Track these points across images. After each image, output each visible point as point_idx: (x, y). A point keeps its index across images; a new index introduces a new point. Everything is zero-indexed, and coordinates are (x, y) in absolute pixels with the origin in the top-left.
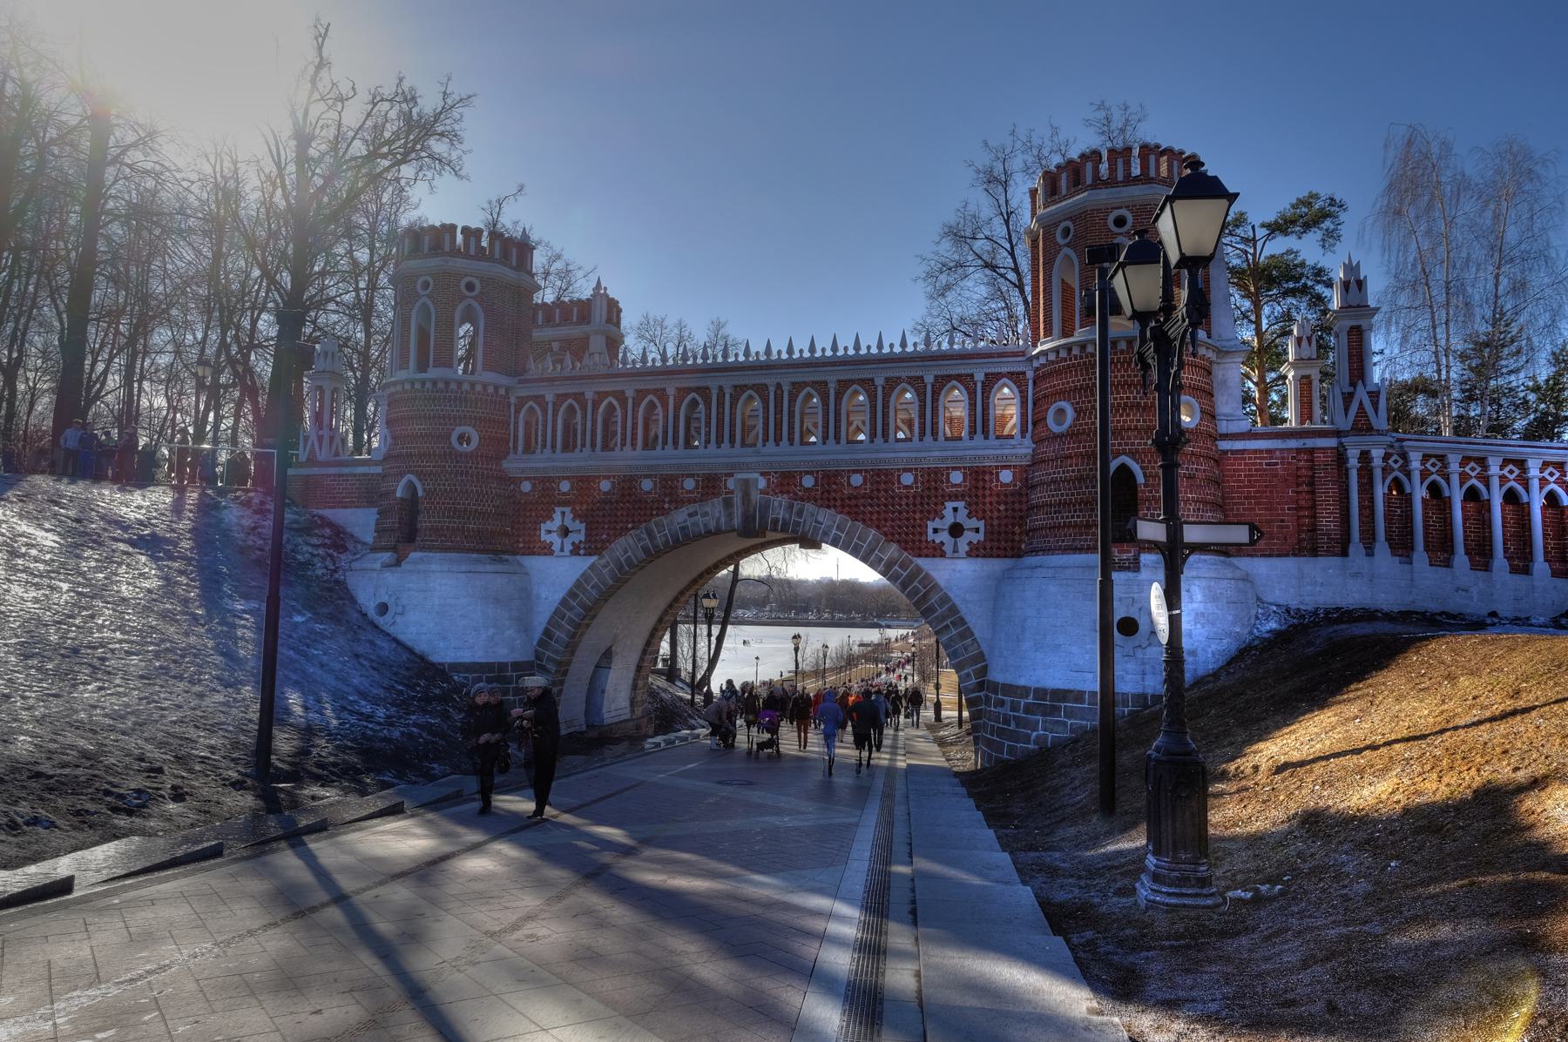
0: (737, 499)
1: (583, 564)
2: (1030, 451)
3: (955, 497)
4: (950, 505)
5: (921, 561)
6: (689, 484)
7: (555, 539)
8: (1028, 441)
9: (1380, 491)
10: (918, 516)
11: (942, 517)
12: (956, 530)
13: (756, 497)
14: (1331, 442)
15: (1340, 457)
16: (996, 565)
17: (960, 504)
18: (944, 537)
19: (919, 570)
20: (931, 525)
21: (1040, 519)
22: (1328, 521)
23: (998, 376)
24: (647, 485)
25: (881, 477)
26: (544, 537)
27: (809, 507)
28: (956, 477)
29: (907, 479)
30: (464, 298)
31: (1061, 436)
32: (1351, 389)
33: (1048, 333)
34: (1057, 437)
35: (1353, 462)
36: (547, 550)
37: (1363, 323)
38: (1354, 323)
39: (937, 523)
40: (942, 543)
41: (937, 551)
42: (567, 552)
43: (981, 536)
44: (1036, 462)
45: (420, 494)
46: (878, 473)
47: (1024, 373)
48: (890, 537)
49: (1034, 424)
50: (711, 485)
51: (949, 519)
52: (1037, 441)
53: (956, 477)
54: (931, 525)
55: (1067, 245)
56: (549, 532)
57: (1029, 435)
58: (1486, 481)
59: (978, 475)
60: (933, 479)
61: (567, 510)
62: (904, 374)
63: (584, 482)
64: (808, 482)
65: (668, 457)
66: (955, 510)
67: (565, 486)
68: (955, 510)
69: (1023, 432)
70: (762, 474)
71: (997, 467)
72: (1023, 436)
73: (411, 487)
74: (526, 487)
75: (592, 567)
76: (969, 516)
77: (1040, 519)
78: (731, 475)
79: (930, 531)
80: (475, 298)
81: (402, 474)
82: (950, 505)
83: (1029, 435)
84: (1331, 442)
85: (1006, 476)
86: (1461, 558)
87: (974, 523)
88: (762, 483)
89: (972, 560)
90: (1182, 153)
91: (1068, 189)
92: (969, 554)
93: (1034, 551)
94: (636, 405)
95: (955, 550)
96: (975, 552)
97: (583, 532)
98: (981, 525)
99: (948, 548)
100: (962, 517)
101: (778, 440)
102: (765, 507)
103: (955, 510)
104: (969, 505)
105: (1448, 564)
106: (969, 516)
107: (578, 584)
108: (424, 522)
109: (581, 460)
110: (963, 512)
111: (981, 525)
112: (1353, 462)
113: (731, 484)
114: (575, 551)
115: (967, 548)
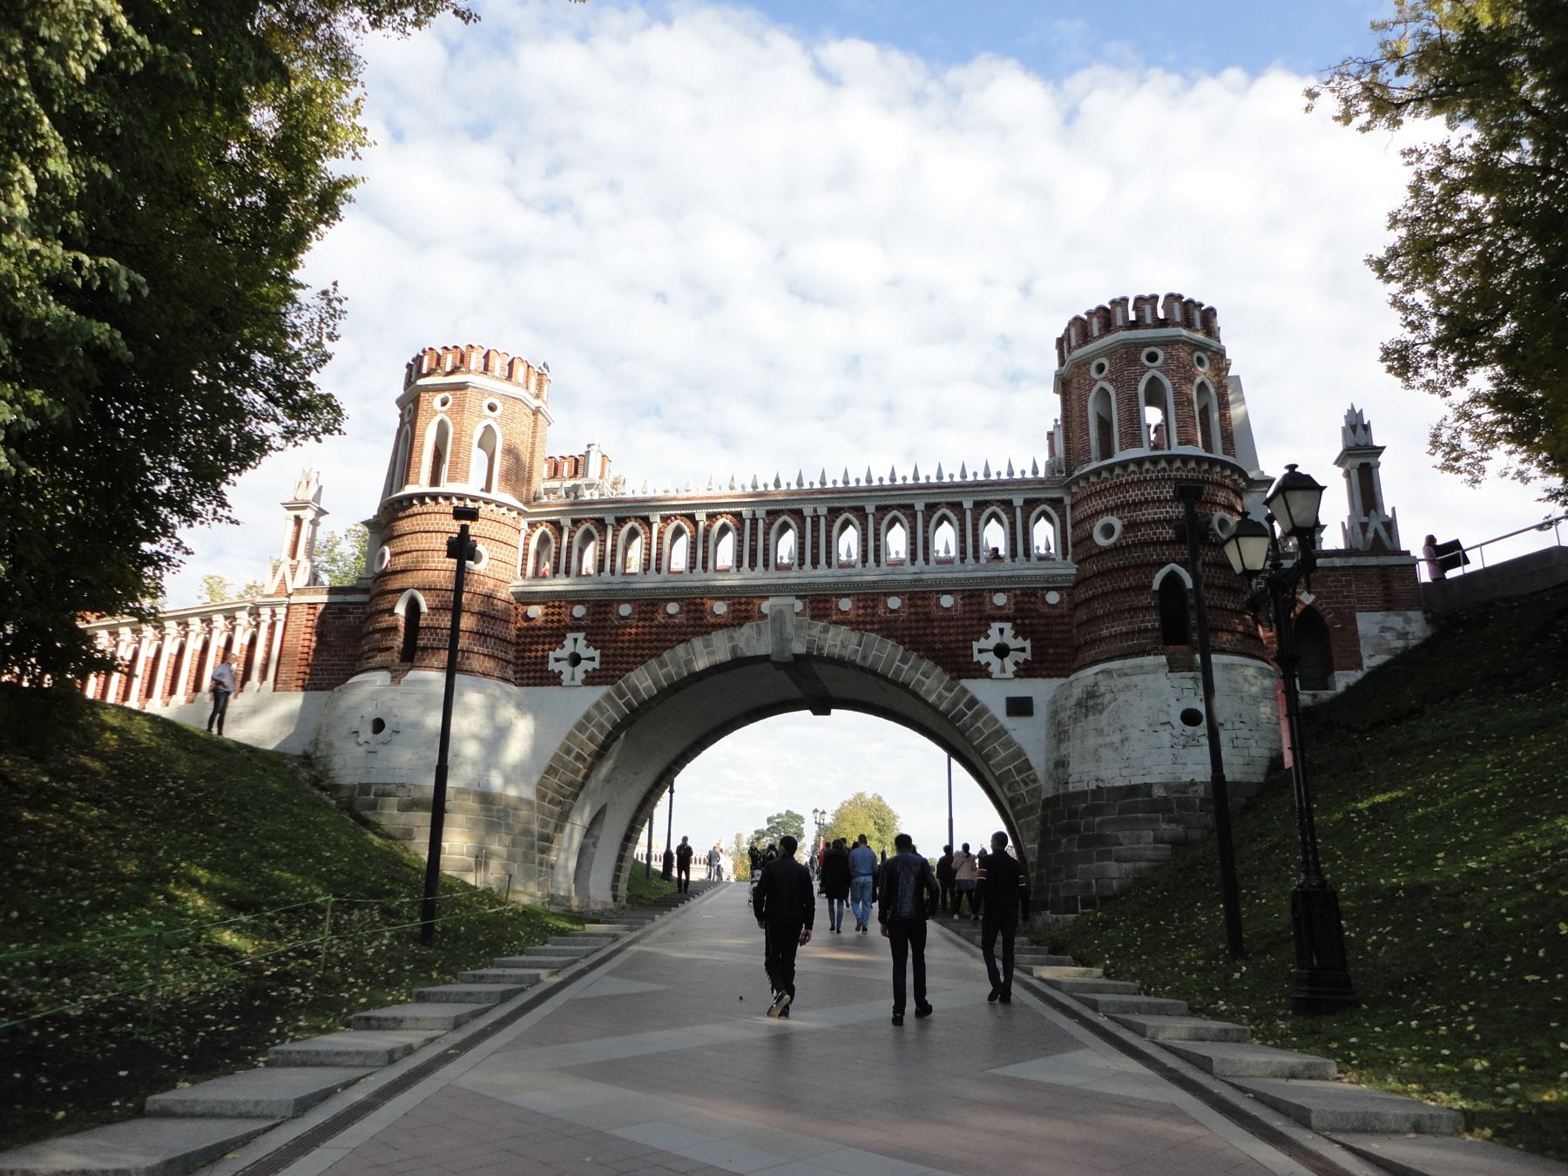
1: (599, 692)
2: (1074, 571)
5: (966, 683)
6: (720, 608)
7: (564, 667)
10: (960, 638)
11: (987, 637)
17: (1007, 626)
18: (990, 657)
19: (964, 691)
20: (976, 646)
24: (672, 608)
26: (553, 666)
29: (947, 601)
30: (486, 417)
32: (1365, 519)
34: (1104, 552)
36: (554, 679)
37: (1370, 460)
38: (1364, 460)
39: (982, 643)
40: (988, 664)
41: (982, 672)
42: (578, 681)
43: (1028, 655)
44: (1081, 581)
45: (424, 608)
47: (1061, 500)
49: (1074, 546)
51: (994, 639)
54: (976, 646)
55: (1103, 379)
56: (557, 660)
57: (1069, 557)
60: (973, 595)
61: (581, 636)
62: (943, 500)
64: (846, 604)
69: (1065, 555)
70: (798, 597)
71: (1042, 589)
72: (1065, 558)
75: (608, 697)
76: (1015, 637)
78: (767, 598)
79: (975, 652)
80: (495, 419)
81: (402, 590)
82: (996, 626)
83: (1069, 557)
88: (799, 605)
89: (1017, 680)
90: (1201, 305)
91: (1100, 329)
92: (1017, 675)
95: (1003, 670)
97: (598, 659)
98: (1027, 644)
101: (815, 562)
103: (1001, 631)
104: (1015, 627)
106: (1015, 637)
107: (588, 717)
111: (1027, 644)
114: (591, 679)
115: (1015, 668)
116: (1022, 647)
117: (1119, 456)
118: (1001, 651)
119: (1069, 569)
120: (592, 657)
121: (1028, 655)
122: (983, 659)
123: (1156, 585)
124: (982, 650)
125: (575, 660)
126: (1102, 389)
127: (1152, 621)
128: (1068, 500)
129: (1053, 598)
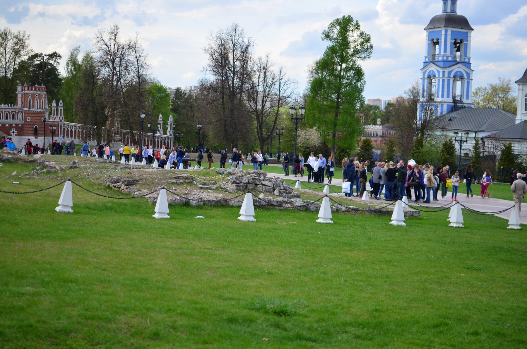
3: (13, 128)
4: (13, 129)
8: (23, 121)
9: (62, 129)
12: (13, 132)
14: (57, 123)
15: (59, 124)
16: (19, 137)
17: (14, 129)
18: (12, 133)
21: (26, 132)
23: (19, 112)
28: (14, 125)
29: (7, 125)
31: (29, 122)
33: (27, 108)
35: (60, 126)
41: (11, 135)
43: (17, 133)
46: (3, 124)
48: (5, 133)
51: (13, 131)
52: (25, 122)
53: (14, 125)
54: (10, 132)
58: (73, 128)
59: (17, 125)
60: (11, 125)
68: (13, 130)
77: (26, 132)
82: (13, 129)
84: (57, 123)
85: (20, 125)
87: (16, 131)
93: (25, 136)
96: (16, 135)
99: (12, 135)
100: (14, 131)
105: (68, 138)
110: (14, 130)
111: (17, 132)
112: (60, 126)
116: (16, 132)
117: (32, 109)
118: (13, 132)
121: (17, 133)
122: (11, 133)
123: (34, 127)
126: (30, 99)
127: (33, 132)
128: (24, 112)
129: (20, 125)
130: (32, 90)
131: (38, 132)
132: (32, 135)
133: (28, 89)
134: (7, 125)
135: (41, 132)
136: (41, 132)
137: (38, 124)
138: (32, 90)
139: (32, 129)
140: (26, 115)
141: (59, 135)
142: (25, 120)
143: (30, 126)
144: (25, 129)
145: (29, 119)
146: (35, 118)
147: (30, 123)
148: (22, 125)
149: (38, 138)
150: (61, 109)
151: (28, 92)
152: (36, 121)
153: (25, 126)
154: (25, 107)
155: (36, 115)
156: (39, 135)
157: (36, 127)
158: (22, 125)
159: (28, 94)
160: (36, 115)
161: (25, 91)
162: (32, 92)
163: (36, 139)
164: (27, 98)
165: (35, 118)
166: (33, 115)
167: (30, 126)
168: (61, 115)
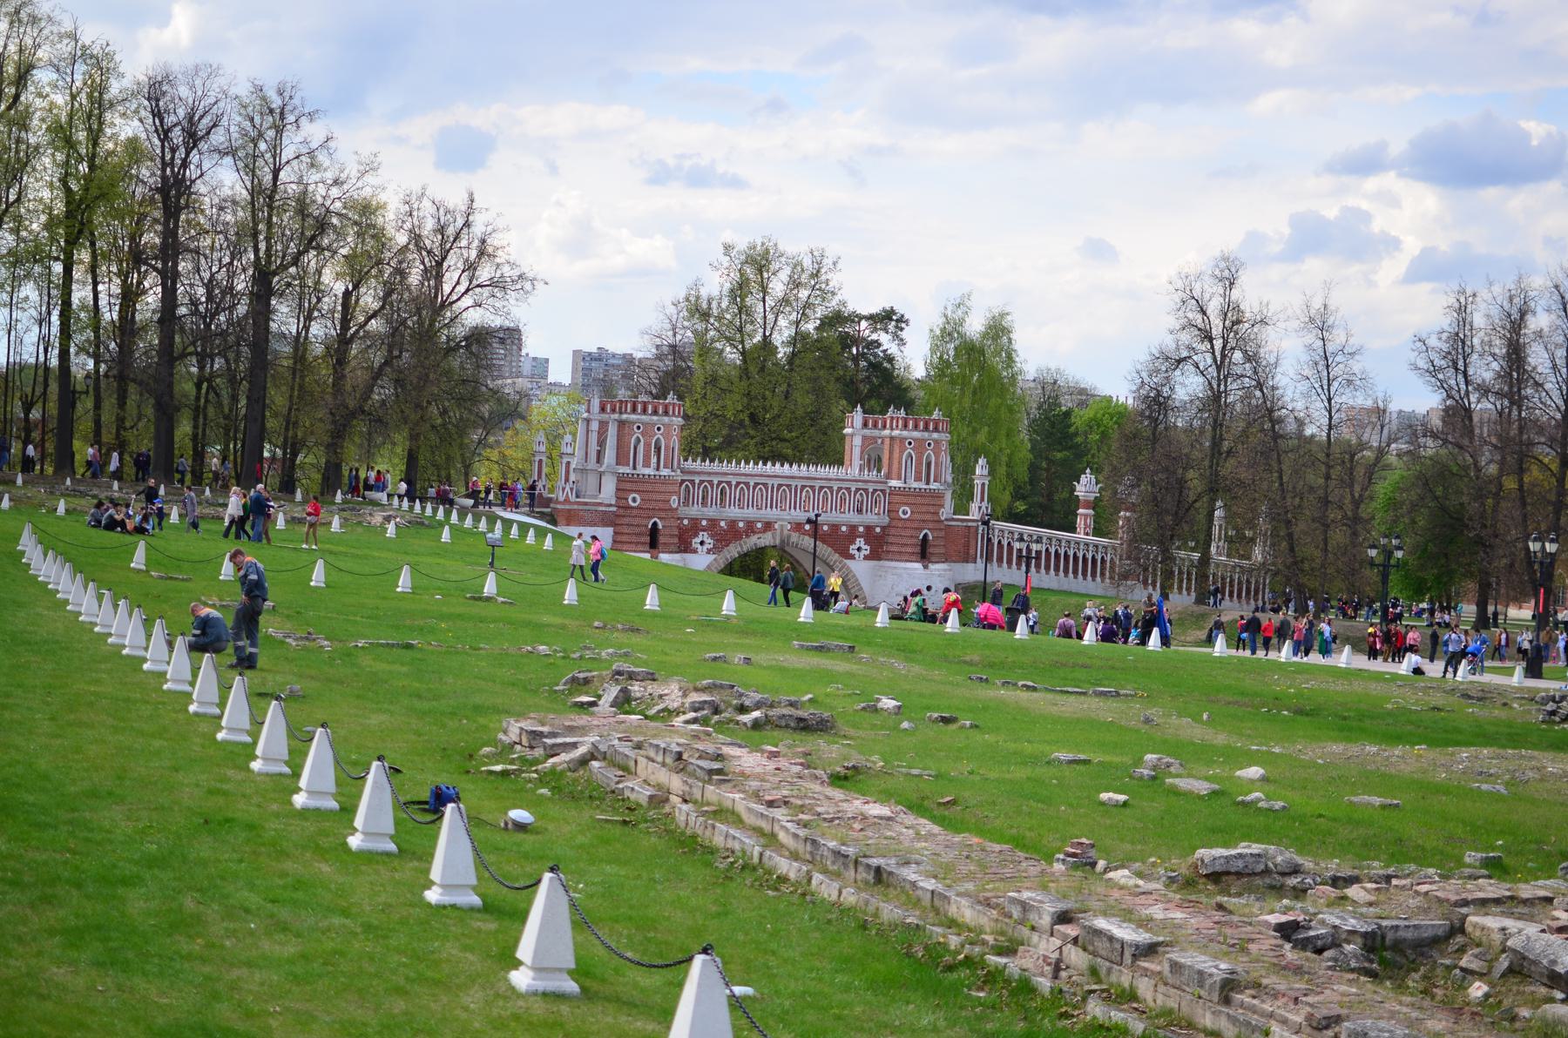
0: (778, 532)
6: (759, 525)
12: (859, 549)
13: (786, 532)
14: (974, 524)
18: (856, 552)
22: (972, 552)
25: (835, 527)
27: (807, 538)
28: (861, 529)
29: (844, 529)
33: (899, 479)
36: (695, 551)
41: (852, 557)
45: (660, 527)
48: (836, 551)
50: (768, 526)
53: (861, 529)
59: (869, 528)
60: (853, 528)
63: (713, 523)
65: (750, 513)
66: (860, 542)
67: (704, 523)
68: (860, 542)
73: (655, 524)
74: (686, 522)
84: (974, 524)
85: (878, 530)
86: (1005, 565)
94: (736, 487)
96: (866, 558)
102: (789, 537)
108: (662, 539)
109: (711, 512)
113: (776, 526)
114: (709, 551)
116: (866, 549)
118: (859, 549)
119: (886, 520)
120: (709, 543)
124: (853, 549)
125: (702, 543)
127: (918, 549)
129: (878, 530)
130: (916, 427)
131: (931, 550)
132: (914, 558)
133: (905, 426)
134: (844, 529)
135: (937, 550)
136: (937, 550)
137: (931, 525)
138: (916, 427)
139: (914, 541)
140: (896, 499)
141: (979, 560)
142: (892, 514)
143: (909, 533)
144: (891, 539)
145: (905, 512)
146: (924, 509)
147: (909, 524)
148: (883, 528)
149: (931, 566)
150: (983, 484)
151: (905, 433)
152: (928, 517)
153: (893, 531)
154: (894, 474)
155: (926, 501)
156: (933, 559)
157: (926, 535)
158: (883, 528)
159: (902, 440)
160: (926, 501)
161: (892, 429)
162: (916, 434)
163: (928, 572)
164: (902, 452)
165: (924, 509)
166: (919, 500)
167: (909, 533)
168: (982, 500)
